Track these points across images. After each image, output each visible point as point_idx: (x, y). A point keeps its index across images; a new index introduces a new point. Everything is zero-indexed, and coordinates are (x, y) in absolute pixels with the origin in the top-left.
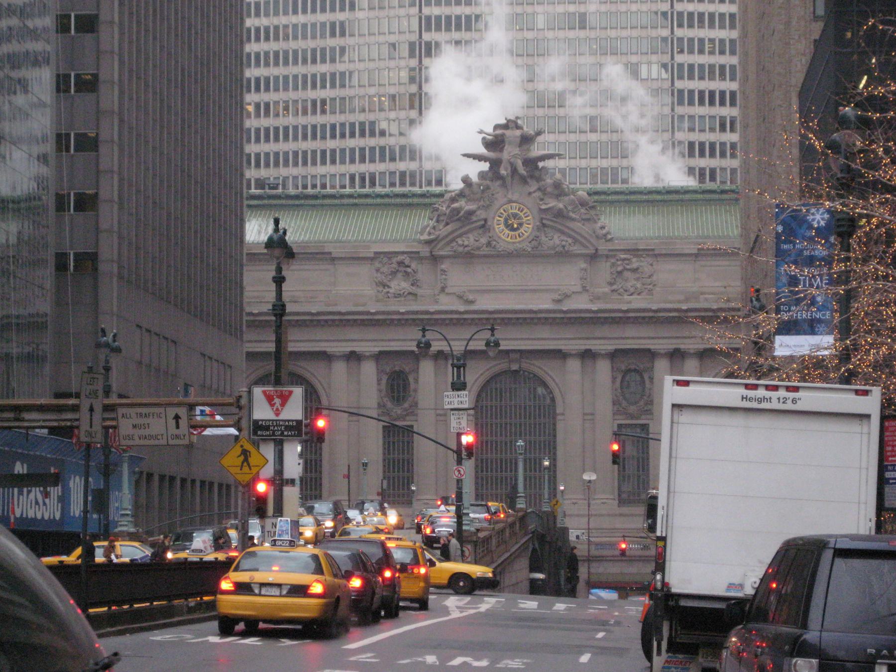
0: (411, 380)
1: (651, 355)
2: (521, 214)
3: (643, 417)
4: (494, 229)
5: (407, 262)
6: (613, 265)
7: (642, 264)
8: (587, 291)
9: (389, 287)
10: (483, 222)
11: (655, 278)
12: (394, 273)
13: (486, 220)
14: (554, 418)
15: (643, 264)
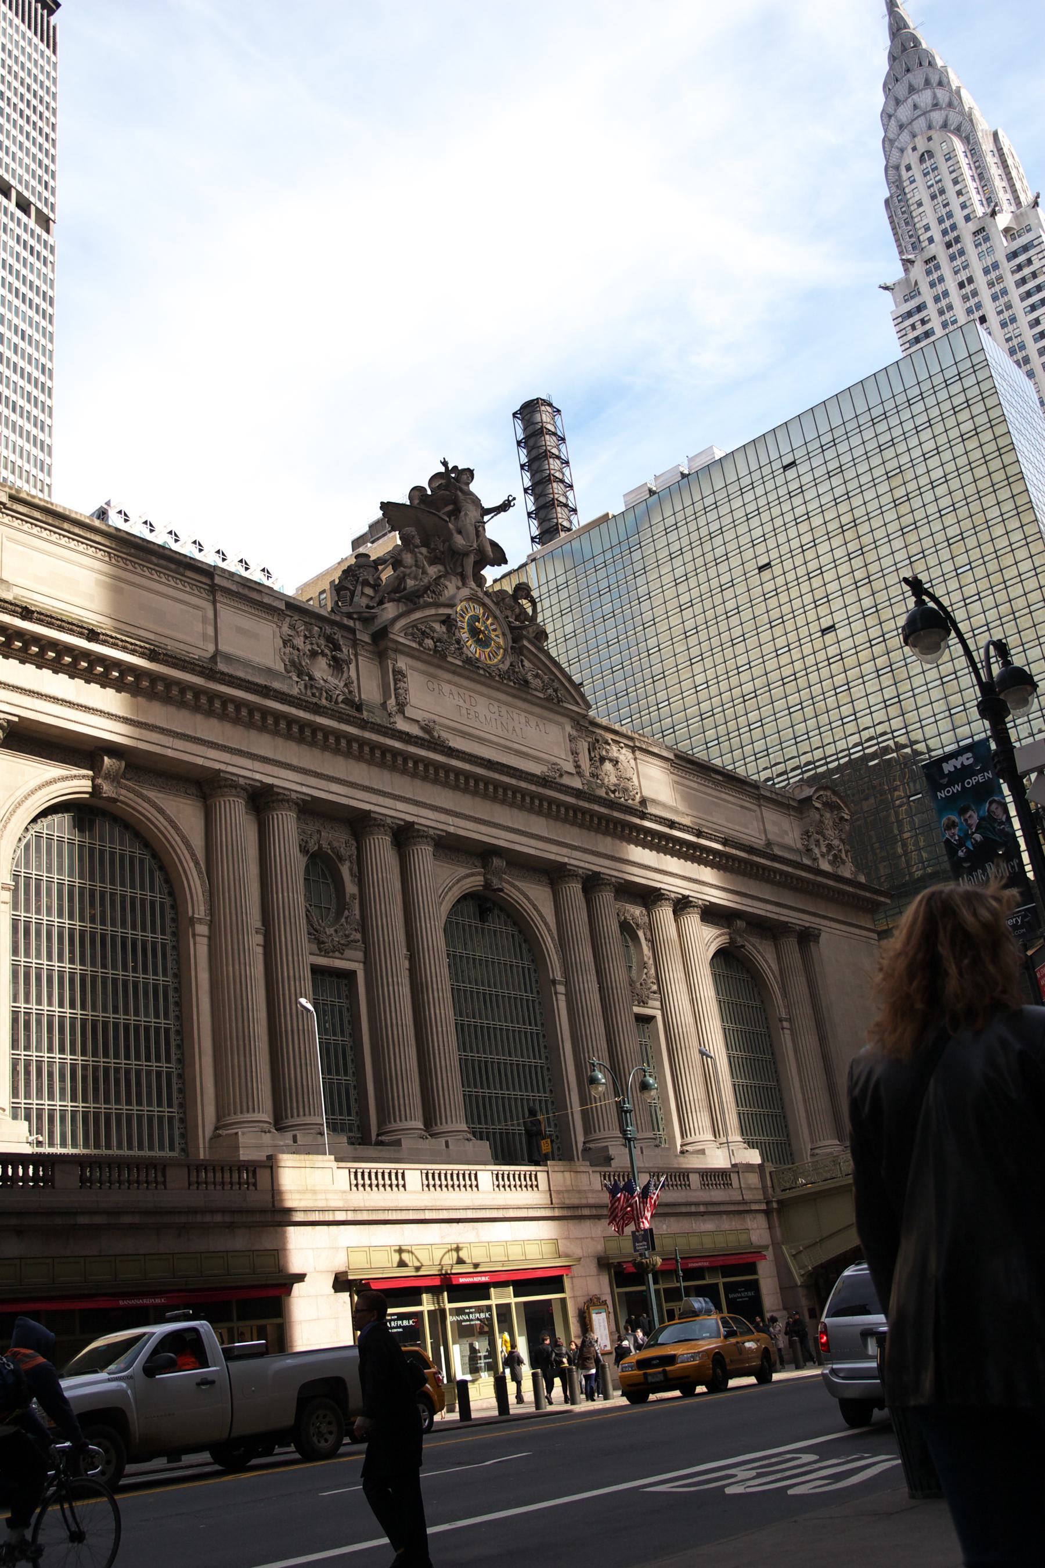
0: (345, 870)
7: (622, 758)
8: (580, 774)
9: (311, 678)
12: (314, 654)
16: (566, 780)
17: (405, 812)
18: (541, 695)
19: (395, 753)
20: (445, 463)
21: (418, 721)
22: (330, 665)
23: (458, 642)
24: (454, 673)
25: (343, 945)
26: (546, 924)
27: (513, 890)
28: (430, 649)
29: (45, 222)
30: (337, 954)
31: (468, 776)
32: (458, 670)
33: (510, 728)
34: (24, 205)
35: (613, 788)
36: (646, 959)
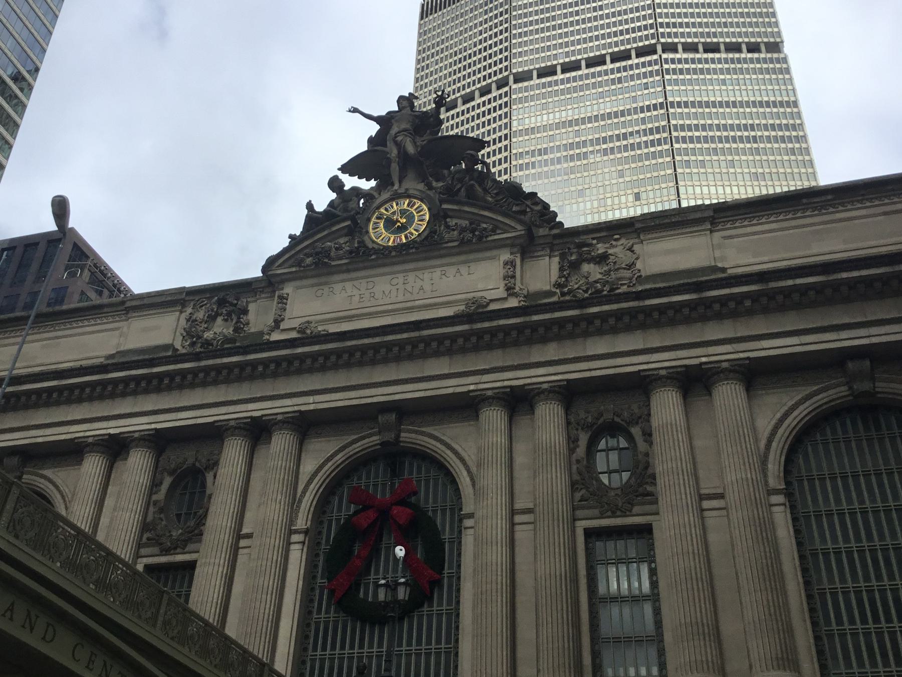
0: (209, 477)
1: (641, 385)
2: (412, 210)
3: (636, 509)
4: (367, 232)
5: (231, 299)
6: (563, 256)
7: (610, 251)
8: (515, 295)
9: (199, 337)
10: (348, 223)
11: (639, 265)
12: (212, 318)
13: (353, 219)
14: (460, 532)
15: (618, 250)
16: (493, 307)
17: (255, 410)
18: (456, 244)
19: (241, 366)
20: (355, 110)
21: (295, 328)
22: (226, 320)
23: (362, 243)
24: (348, 271)
25: (184, 541)
26: (462, 460)
27: (420, 437)
28: (308, 266)
29: (775, 47)
30: (178, 550)
31: (326, 355)
32: (350, 267)
33: (416, 290)
34: (753, 48)
35: (584, 288)
36: (640, 457)
